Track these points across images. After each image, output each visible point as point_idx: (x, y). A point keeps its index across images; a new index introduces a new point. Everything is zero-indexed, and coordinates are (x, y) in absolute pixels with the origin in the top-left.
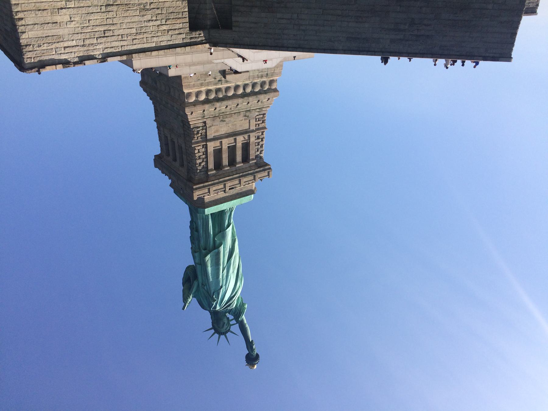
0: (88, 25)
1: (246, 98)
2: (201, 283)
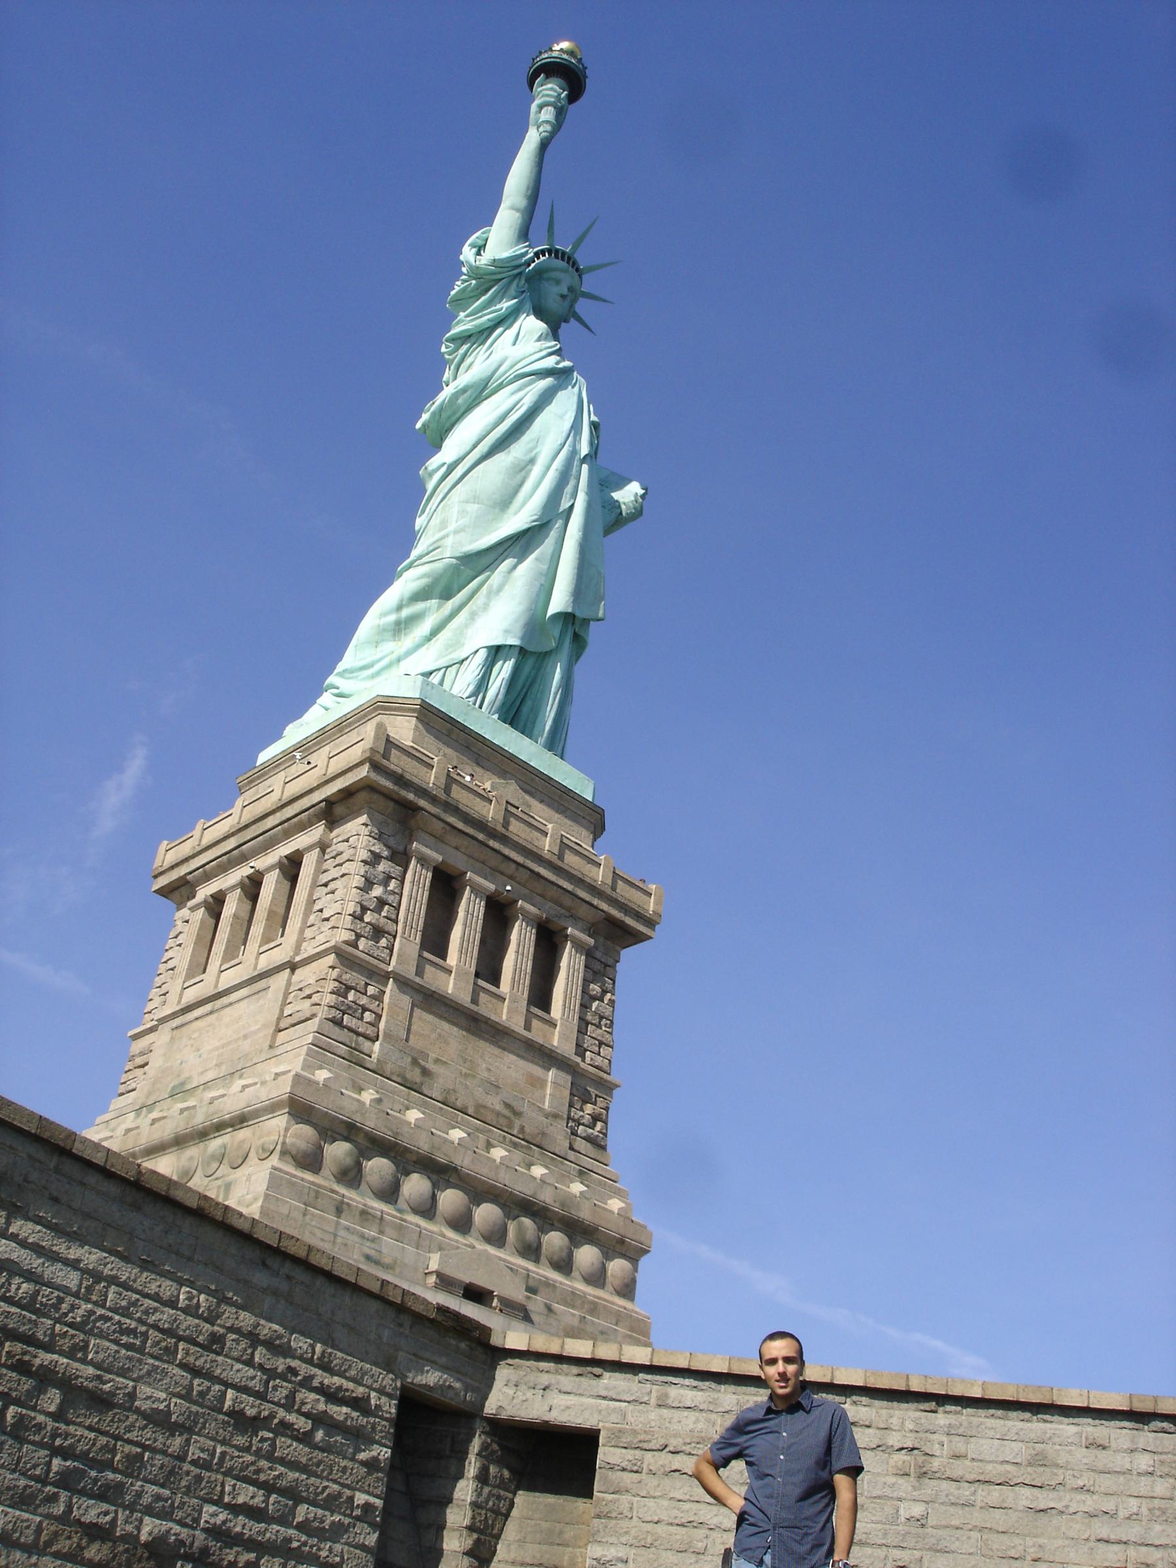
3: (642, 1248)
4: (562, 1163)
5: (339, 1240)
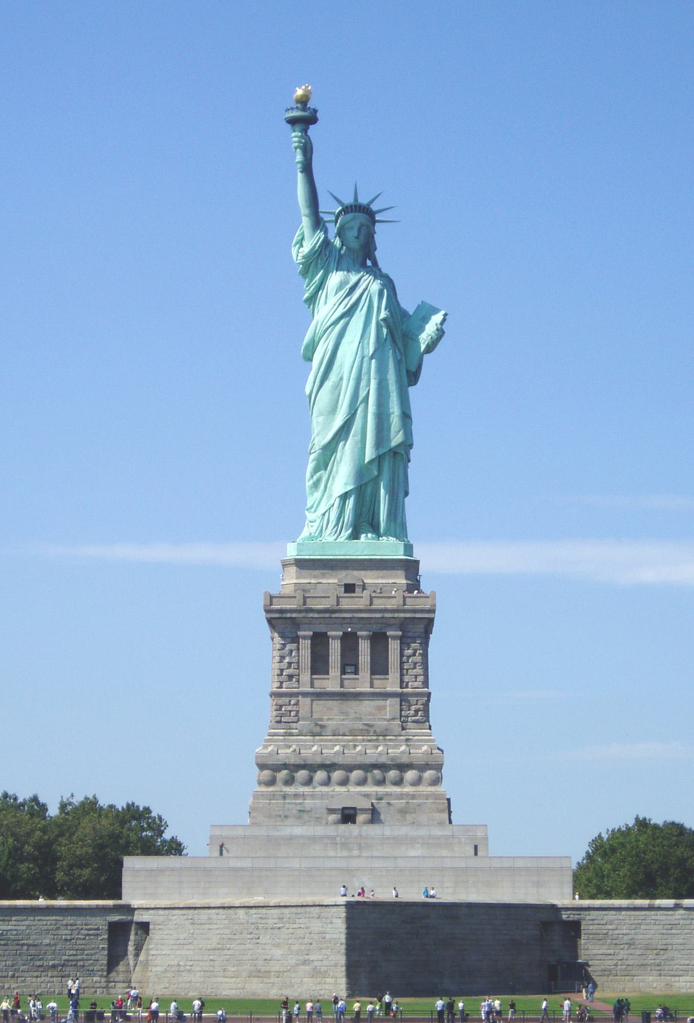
0: (686, 936)
5: (286, 808)
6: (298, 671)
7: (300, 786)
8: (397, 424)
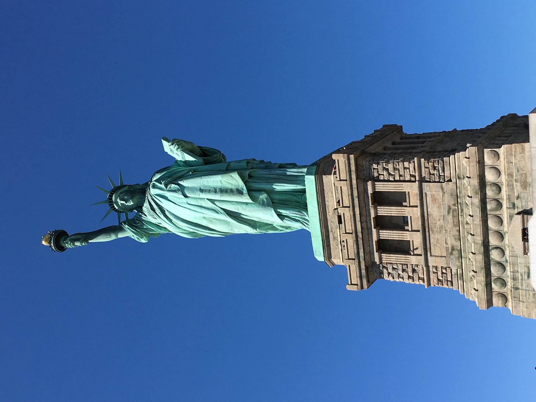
1: (482, 249)
2: (197, 169)
3: (478, 152)
4: (459, 188)
5: (527, 288)
6: (408, 265)
7: (506, 272)
8: (227, 178)
